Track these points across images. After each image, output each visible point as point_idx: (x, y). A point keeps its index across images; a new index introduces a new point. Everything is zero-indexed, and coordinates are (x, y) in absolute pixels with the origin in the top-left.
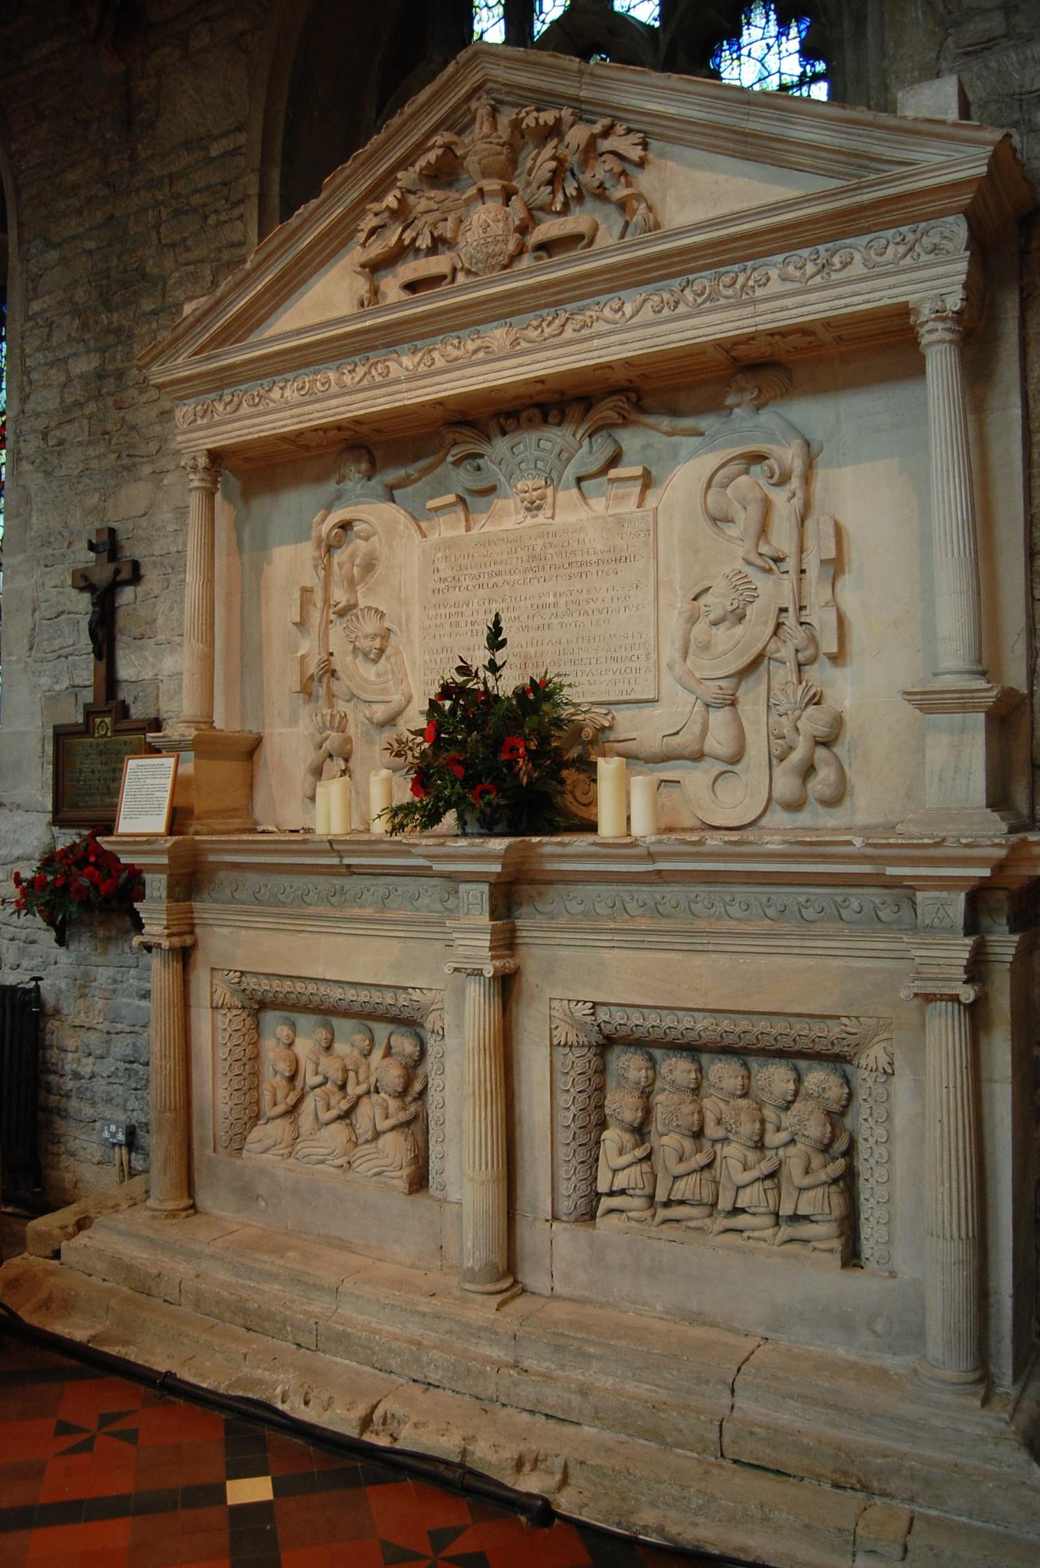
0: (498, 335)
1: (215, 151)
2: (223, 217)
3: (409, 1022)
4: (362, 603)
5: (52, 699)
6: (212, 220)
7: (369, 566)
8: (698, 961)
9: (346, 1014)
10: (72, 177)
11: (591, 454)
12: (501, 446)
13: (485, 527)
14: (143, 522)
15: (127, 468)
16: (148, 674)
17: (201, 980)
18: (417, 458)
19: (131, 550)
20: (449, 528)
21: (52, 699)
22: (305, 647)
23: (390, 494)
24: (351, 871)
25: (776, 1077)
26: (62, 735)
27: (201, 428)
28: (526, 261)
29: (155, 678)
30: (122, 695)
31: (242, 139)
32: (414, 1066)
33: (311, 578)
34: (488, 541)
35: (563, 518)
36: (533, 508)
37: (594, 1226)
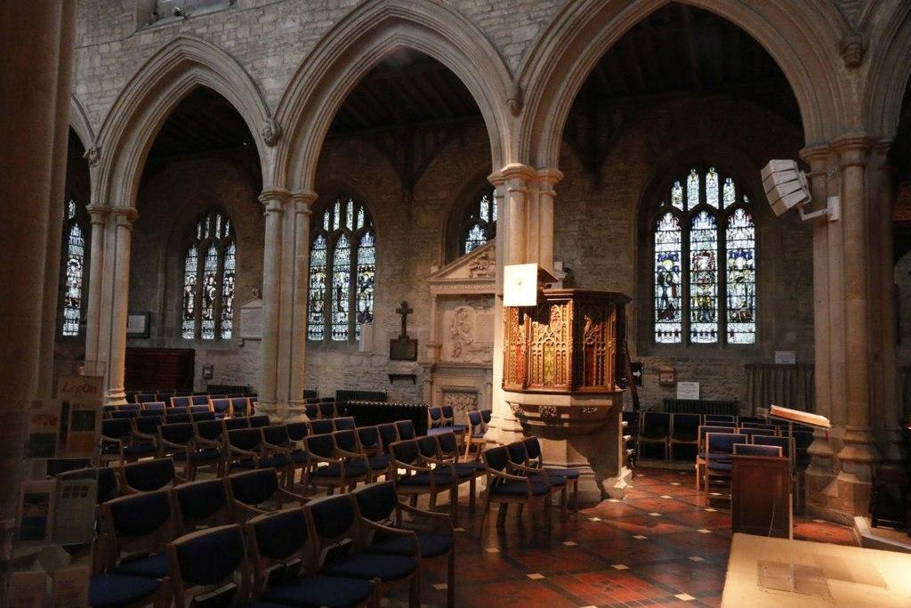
1: (431, 231)
3: (475, 393)
5: (389, 334)
7: (466, 316)
9: (461, 392)
10: (395, 227)
15: (410, 289)
17: (434, 387)
19: (410, 307)
20: (481, 312)
21: (389, 334)
22: (452, 330)
23: (470, 305)
24: (465, 368)
26: (393, 342)
29: (416, 332)
30: (407, 334)
31: (437, 231)
32: (475, 400)
34: (488, 315)
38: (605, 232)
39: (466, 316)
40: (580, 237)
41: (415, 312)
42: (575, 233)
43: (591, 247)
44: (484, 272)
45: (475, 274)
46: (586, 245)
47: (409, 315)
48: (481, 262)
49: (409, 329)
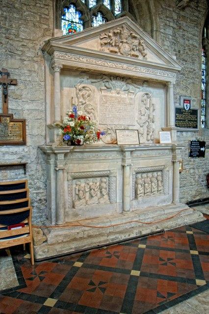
0: (125, 66)
2: (42, 6)
4: (87, 103)
6: (38, 5)
8: (151, 160)
11: (124, 87)
12: (114, 82)
13: (109, 94)
14: (17, 70)
15: (12, 53)
16: (20, 108)
18: (96, 79)
25: (155, 174)
27: (62, 59)
28: (129, 56)
33: (74, 95)
35: (123, 96)
36: (118, 93)
37: (137, 199)
38: (187, 42)
39: (89, 96)
40: (173, 41)
41: (21, 85)
42: (170, 37)
43: (179, 52)
44: (116, 49)
45: (106, 50)
46: (176, 48)
47: (12, 87)
48: (114, 38)
49: (12, 105)
